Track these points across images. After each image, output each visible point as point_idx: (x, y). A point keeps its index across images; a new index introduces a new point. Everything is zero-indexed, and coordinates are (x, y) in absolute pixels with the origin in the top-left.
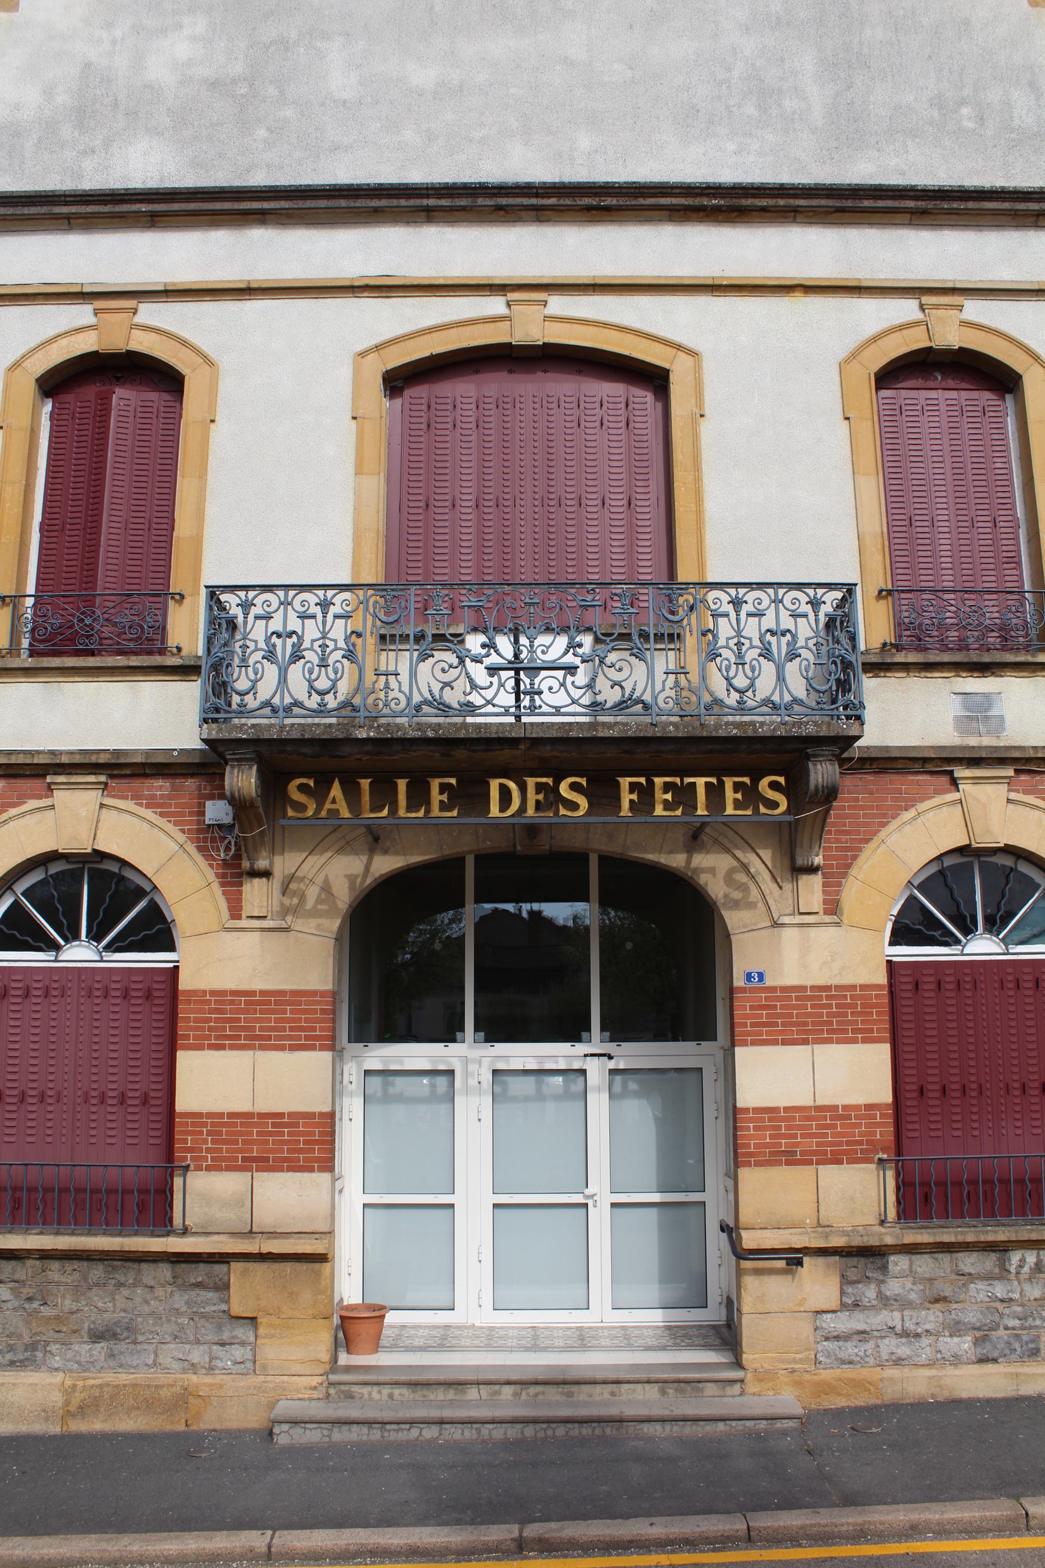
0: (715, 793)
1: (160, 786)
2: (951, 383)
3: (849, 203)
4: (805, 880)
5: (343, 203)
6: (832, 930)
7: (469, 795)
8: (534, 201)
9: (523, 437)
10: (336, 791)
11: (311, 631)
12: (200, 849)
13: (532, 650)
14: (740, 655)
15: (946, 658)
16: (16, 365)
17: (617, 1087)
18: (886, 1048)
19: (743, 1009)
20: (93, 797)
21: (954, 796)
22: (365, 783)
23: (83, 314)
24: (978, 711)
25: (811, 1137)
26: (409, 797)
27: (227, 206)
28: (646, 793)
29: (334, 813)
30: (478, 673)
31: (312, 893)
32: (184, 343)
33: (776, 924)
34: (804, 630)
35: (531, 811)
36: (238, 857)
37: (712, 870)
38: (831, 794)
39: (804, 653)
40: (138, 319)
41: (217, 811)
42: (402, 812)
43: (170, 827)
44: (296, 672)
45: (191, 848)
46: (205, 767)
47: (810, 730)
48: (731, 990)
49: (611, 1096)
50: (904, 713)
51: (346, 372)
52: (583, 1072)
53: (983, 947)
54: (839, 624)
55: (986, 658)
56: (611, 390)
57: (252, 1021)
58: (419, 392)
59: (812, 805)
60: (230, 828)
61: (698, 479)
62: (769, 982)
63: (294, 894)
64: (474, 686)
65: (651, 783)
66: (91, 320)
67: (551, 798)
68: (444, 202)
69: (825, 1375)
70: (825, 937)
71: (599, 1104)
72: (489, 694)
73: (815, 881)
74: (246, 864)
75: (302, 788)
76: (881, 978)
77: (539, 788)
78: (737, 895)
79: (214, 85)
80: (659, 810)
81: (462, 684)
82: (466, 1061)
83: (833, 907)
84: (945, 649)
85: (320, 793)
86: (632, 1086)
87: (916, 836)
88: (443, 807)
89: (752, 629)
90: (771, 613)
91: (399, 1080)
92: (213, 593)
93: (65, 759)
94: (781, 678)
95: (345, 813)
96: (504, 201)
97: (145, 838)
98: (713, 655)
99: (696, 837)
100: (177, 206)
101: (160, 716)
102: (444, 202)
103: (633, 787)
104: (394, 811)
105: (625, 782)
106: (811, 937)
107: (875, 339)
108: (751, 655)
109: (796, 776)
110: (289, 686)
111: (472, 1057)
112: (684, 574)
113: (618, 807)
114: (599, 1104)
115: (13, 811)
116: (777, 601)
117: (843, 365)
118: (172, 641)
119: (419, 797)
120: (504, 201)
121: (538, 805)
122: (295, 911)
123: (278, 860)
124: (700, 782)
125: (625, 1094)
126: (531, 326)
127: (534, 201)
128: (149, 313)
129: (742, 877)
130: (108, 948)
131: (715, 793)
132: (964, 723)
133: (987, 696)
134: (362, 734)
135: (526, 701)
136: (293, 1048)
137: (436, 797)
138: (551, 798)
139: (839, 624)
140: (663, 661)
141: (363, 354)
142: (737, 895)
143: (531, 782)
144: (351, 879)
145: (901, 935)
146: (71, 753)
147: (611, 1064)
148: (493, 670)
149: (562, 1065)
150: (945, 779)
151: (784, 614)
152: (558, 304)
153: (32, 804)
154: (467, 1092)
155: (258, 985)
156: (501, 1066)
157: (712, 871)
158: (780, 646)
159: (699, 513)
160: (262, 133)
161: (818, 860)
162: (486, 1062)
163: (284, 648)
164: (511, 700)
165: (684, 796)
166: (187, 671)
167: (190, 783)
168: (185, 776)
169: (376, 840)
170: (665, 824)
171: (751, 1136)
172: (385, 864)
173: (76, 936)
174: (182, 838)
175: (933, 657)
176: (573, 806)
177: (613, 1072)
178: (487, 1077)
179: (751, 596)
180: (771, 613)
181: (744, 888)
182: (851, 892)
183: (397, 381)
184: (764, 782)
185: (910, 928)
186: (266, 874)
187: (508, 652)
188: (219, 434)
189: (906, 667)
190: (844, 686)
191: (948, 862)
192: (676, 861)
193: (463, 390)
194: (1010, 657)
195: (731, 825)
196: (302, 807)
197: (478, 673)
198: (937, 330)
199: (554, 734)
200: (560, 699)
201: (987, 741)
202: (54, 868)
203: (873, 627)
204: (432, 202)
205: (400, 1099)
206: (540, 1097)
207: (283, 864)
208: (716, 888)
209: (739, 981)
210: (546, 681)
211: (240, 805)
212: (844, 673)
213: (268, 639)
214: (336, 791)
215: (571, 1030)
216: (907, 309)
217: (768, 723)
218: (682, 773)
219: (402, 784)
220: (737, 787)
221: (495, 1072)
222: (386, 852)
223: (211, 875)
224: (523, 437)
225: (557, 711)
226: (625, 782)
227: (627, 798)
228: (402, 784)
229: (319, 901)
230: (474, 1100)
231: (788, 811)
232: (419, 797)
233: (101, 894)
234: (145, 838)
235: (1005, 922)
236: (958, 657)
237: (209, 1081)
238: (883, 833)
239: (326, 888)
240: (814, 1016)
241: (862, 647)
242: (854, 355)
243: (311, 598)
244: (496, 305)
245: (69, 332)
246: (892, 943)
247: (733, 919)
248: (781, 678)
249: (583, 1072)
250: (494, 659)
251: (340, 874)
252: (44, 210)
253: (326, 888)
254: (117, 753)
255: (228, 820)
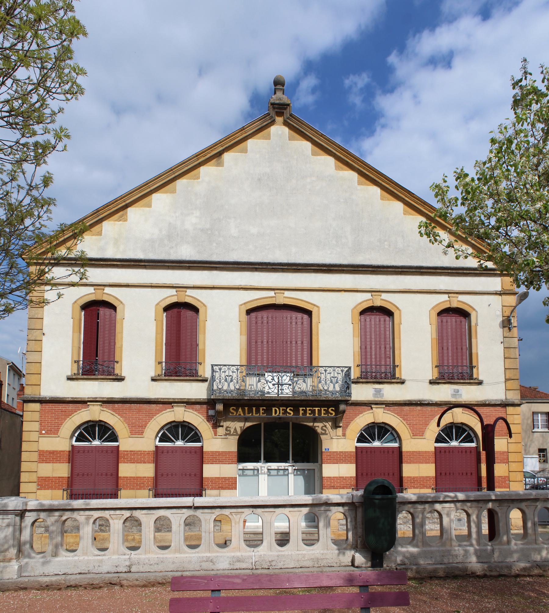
0: (320, 411)
1: (198, 406)
2: (378, 313)
3: (356, 269)
4: (338, 429)
5: (236, 266)
6: (344, 440)
7: (268, 411)
8: (282, 267)
9: (280, 328)
10: (240, 410)
11: (235, 375)
12: (207, 421)
13: (282, 381)
14: (326, 382)
15: (371, 380)
16: (158, 304)
17: (295, 473)
18: (354, 465)
19: (324, 456)
20: (183, 409)
21: (371, 411)
22: (246, 408)
23: (173, 292)
24: (378, 391)
25: (338, 483)
26: (256, 411)
27: (208, 265)
28: (305, 411)
29: (240, 415)
30: (271, 386)
31: (232, 431)
32: (199, 300)
33: (332, 438)
34: (340, 377)
35: (281, 415)
36: (216, 422)
37: (318, 426)
38: (344, 412)
39: (340, 382)
40: (187, 294)
41: (211, 412)
42: (254, 415)
43: (200, 416)
44: (231, 384)
45: (205, 420)
46: (210, 403)
47: (340, 398)
48: (322, 452)
49: (294, 475)
50: (361, 392)
51: (237, 309)
52: (288, 469)
53: (377, 444)
54: (348, 374)
55: (380, 381)
56: (299, 315)
57: (219, 458)
58: (253, 315)
59: (340, 414)
60: (214, 416)
61: (318, 338)
62: (330, 450)
63: (228, 431)
64: (270, 388)
65: (306, 409)
66: (176, 293)
67: (285, 412)
68: (260, 267)
69: (340, 532)
70: (342, 441)
71: (291, 477)
72: (273, 390)
73: (341, 429)
74: (218, 424)
75: (233, 409)
76: (354, 450)
77: (283, 410)
78: (324, 432)
79: (202, 230)
80: (308, 415)
81: (267, 388)
82: (261, 467)
83: (344, 435)
84: (371, 378)
85: (237, 411)
86: (299, 473)
87: (364, 419)
88: (263, 413)
89: (328, 376)
90: (333, 373)
91: (246, 471)
92: (212, 366)
93: (176, 400)
94: (334, 387)
95: (242, 415)
96: (274, 267)
97: (197, 419)
98: (320, 382)
99: (315, 420)
100: (195, 265)
101: (197, 391)
102: (260, 267)
103: (303, 410)
104: (252, 414)
105: (301, 409)
106: (339, 442)
107: (360, 303)
108: (328, 382)
109: (336, 408)
110: (229, 385)
111: (262, 466)
112: (314, 364)
113: (299, 414)
114: (291, 477)
115: (164, 412)
116: (334, 370)
117: (353, 310)
118: (199, 374)
119: (258, 411)
120: (274, 267)
121: (283, 413)
122: (229, 434)
123: (225, 423)
124: (317, 409)
125: (297, 475)
126: (281, 300)
127: (282, 267)
128: (189, 292)
129: (324, 428)
130: (186, 442)
131: (320, 411)
132: (375, 395)
133: (380, 389)
134: (246, 398)
135: (280, 391)
136: (229, 464)
137: (261, 411)
138: (285, 412)
139: (348, 374)
140: (309, 381)
141: (241, 305)
142: (324, 432)
143: (281, 408)
144: (241, 427)
145: (359, 441)
146: (178, 399)
147: (294, 468)
148: (274, 385)
149: (283, 468)
150: (370, 407)
151: (336, 373)
152: (287, 294)
153: (168, 410)
154: (262, 474)
155: (221, 450)
156: (269, 468)
157: (318, 427)
158: (334, 380)
159: (318, 346)
160: (215, 244)
161: (341, 425)
162: (266, 467)
163: (229, 379)
164: (277, 391)
165: (313, 412)
166: (205, 380)
167: (205, 406)
168: (203, 404)
169: (246, 420)
170: (309, 418)
171: (325, 483)
172: (248, 424)
173: (179, 439)
174: (203, 418)
175: (368, 380)
176: (290, 414)
177: (295, 469)
178: (266, 470)
179: (329, 369)
180: (333, 373)
181: (325, 431)
182: (348, 432)
183: (249, 312)
184: (330, 409)
185: (361, 439)
186: (222, 426)
187: (277, 381)
188: (208, 324)
189: (362, 383)
190: (348, 388)
191: (370, 425)
192: (311, 424)
193: (264, 314)
194: (386, 380)
195: (324, 418)
196: (233, 413)
197: (271, 385)
198: (375, 301)
199: (286, 399)
200: (287, 391)
201: (380, 399)
202: (173, 424)
203: (355, 374)
204: (257, 267)
205: (246, 475)
206: (278, 475)
207: (226, 424)
208: (319, 430)
209: (324, 450)
210: (285, 387)
211: (218, 413)
212: (347, 387)
213: (225, 377)
214: (240, 410)
215: (285, 460)
216: (368, 296)
217: (330, 397)
218: (313, 407)
219: (254, 409)
220: (324, 410)
221: (268, 469)
222: (248, 422)
223: (210, 426)
224: (280, 328)
225: (287, 394)
226: (301, 409)
227: (301, 412)
228: (254, 409)
229: (234, 432)
230: (263, 476)
231: (335, 415)
232: (258, 411)
233: (187, 431)
234: (197, 419)
235: (382, 439)
236: (374, 380)
237: (210, 471)
238: (356, 419)
239: (235, 429)
240: (339, 458)
241: (352, 378)
242: (355, 307)
243: (234, 368)
244: (272, 293)
245: (170, 296)
246: (357, 442)
247: (322, 437)
248: (334, 387)
249: (288, 469)
250: (274, 382)
251: (238, 426)
252: (162, 264)
253: (235, 429)
254: (188, 399)
255: (214, 414)
